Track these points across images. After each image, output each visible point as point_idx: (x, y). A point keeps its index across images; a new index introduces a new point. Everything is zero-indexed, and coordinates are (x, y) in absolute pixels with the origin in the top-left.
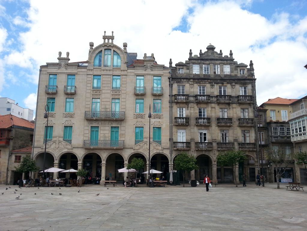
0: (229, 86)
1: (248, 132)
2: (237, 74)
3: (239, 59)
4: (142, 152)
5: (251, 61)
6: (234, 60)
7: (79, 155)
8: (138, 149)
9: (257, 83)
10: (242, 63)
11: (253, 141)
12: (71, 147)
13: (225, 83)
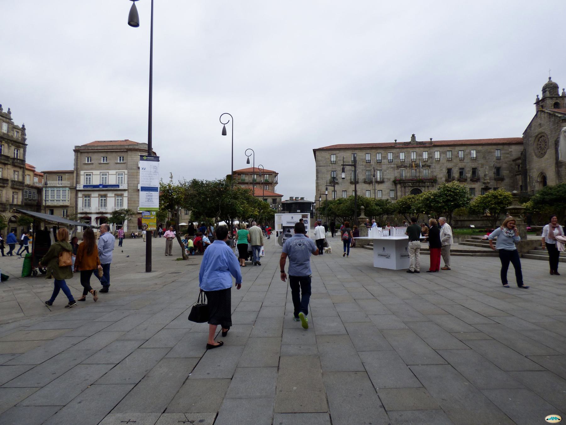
0: (6, 145)
1: (16, 194)
2: (13, 135)
3: (17, 121)
5: (23, 126)
6: (12, 119)
9: (28, 148)
10: (17, 125)
11: (20, 203)
13: (4, 142)
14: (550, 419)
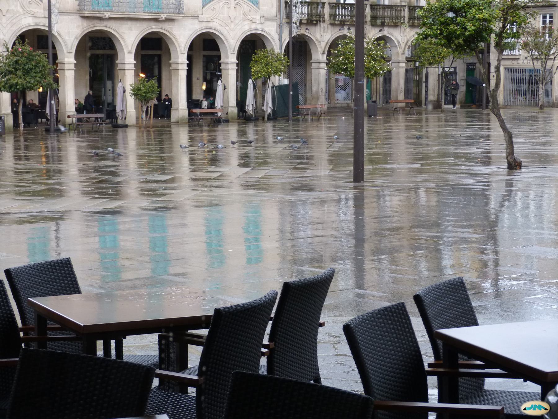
4: (219, 28)
7: (67, 38)
8: (209, 20)
12: (42, 11)
14: (530, 408)
